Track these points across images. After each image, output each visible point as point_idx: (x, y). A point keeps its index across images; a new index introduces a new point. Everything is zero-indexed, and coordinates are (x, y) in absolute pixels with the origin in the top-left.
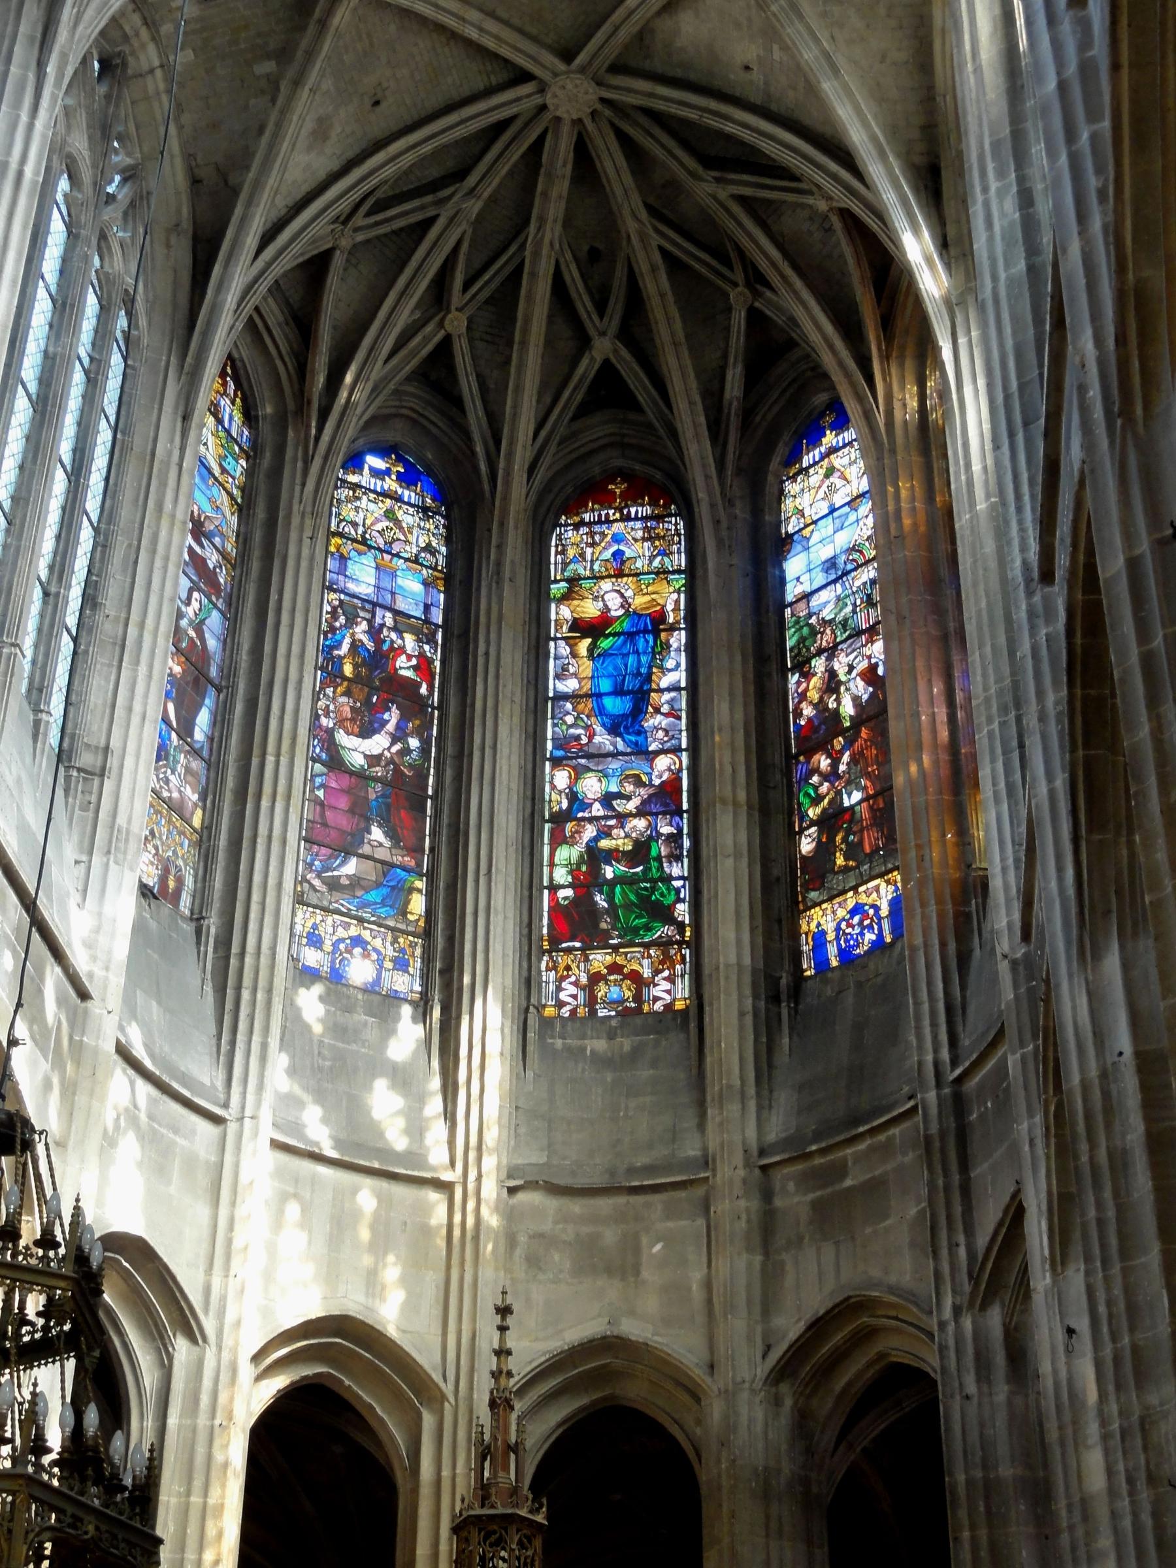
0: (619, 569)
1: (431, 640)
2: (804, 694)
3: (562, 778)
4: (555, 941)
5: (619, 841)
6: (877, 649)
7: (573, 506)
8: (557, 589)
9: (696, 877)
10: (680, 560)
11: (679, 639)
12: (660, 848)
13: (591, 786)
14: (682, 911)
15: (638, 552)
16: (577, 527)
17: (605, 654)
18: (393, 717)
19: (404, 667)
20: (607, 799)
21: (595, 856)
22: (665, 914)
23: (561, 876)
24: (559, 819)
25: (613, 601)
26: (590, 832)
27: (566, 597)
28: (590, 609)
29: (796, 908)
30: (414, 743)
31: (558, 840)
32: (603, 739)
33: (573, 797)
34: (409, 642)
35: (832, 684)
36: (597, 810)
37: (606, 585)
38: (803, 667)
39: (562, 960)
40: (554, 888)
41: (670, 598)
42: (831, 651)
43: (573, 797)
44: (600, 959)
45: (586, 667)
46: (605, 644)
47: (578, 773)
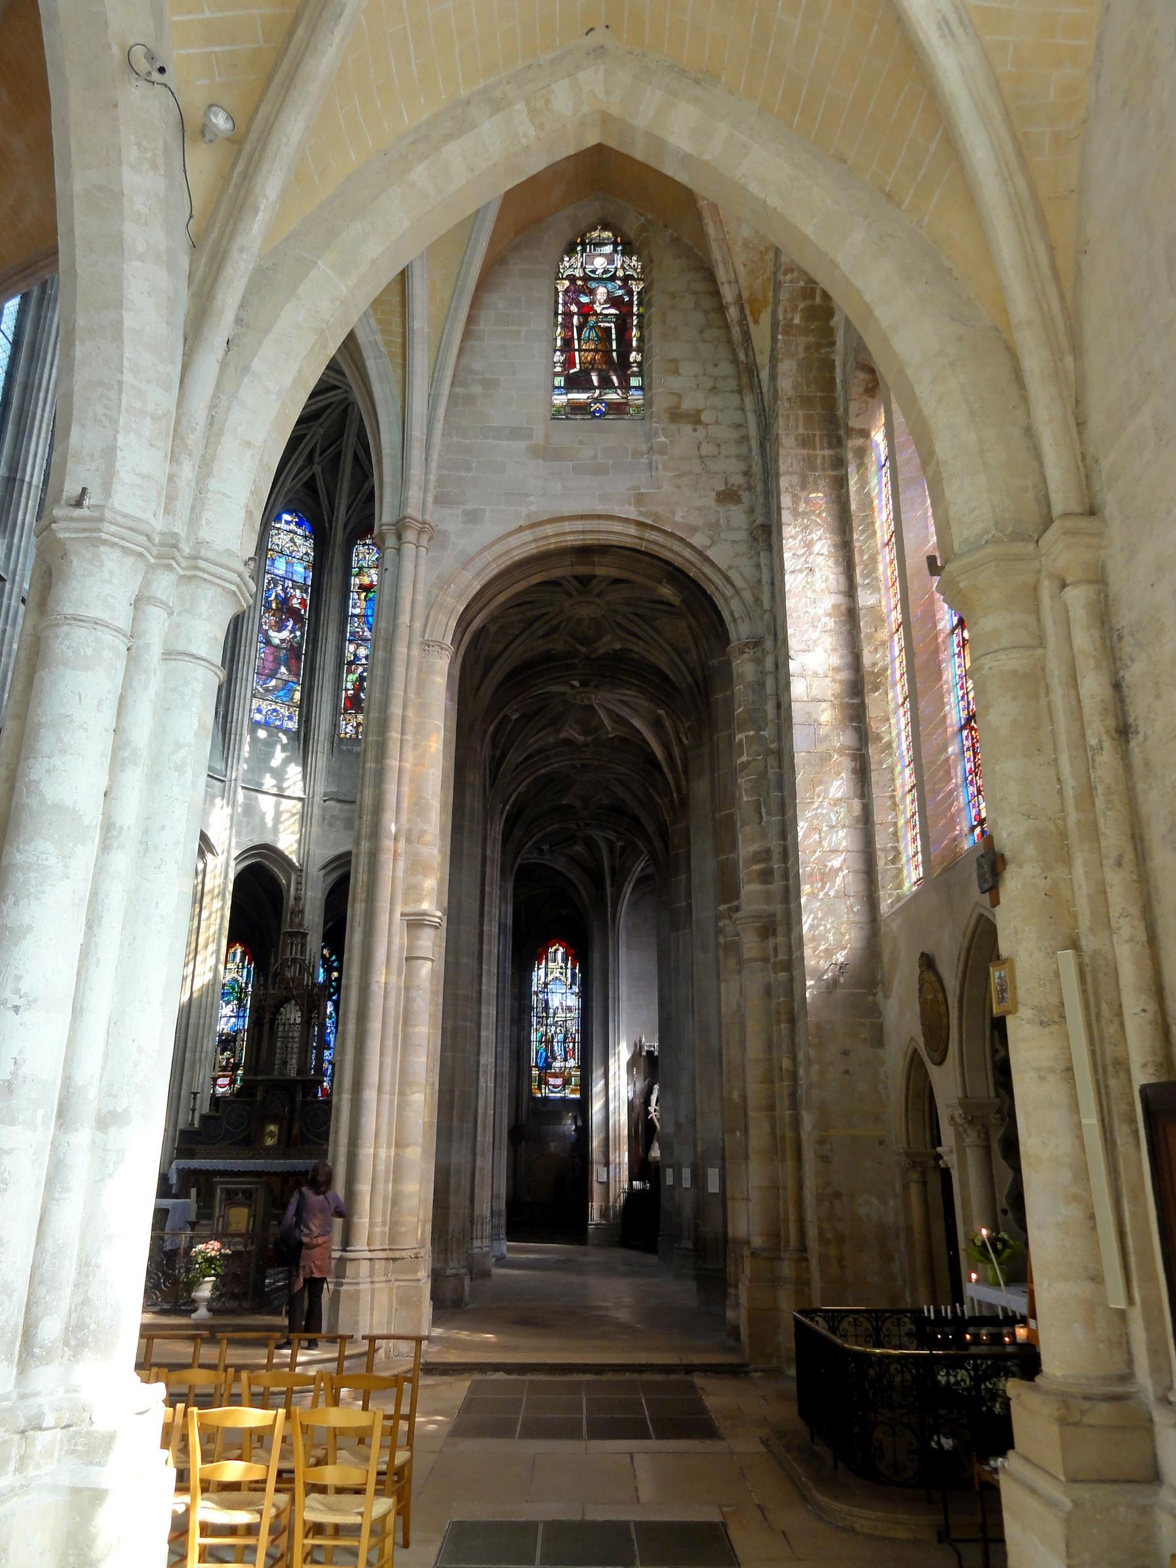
1: (306, 592)
3: (352, 648)
4: (346, 710)
8: (355, 571)
16: (364, 545)
17: (371, 599)
18: (290, 624)
19: (295, 603)
20: (366, 657)
21: (361, 679)
23: (349, 685)
24: (350, 663)
25: (375, 578)
26: (360, 669)
27: (358, 575)
28: (366, 581)
30: (298, 633)
31: (349, 672)
32: (367, 634)
33: (355, 655)
34: (298, 592)
36: (364, 661)
37: (373, 571)
39: (348, 717)
40: (347, 690)
43: (355, 655)
44: (360, 717)
45: (364, 604)
46: (371, 595)
47: (358, 646)
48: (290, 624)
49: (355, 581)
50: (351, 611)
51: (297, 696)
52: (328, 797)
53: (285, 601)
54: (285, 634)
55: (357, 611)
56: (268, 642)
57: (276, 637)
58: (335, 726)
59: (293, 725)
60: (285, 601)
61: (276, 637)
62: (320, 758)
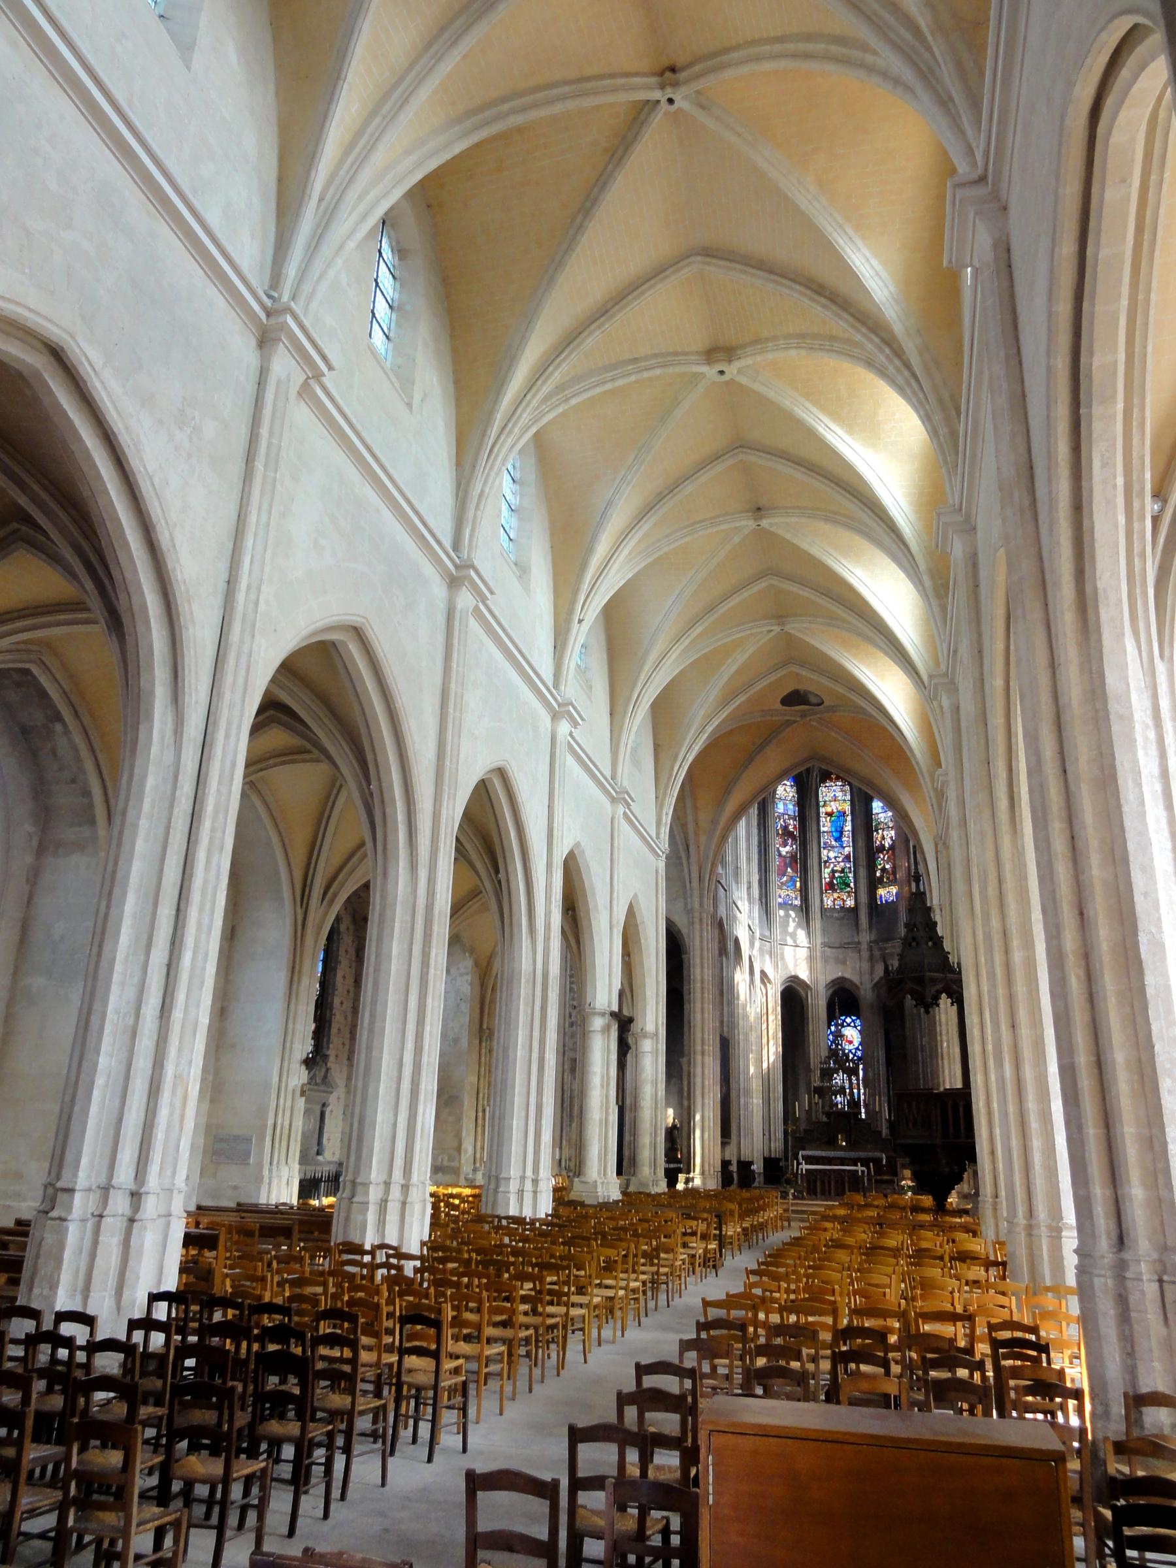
0: (835, 799)
2: (877, 836)
5: (838, 868)
6: (893, 833)
7: (824, 782)
8: (821, 804)
9: (855, 877)
10: (848, 797)
11: (849, 818)
12: (847, 870)
13: (832, 855)
14: (852, 885)
15: (839, 794)
18: (790, 841)
21: (833, 871)
22: (848, 885)
24: (826, 862)
28: (829, 810)
29: (876, 888)
32: (833, 843)
35: (883, 838)
38: (877, 831)
41: (847, 807)
42: (883, 830)
44: (836, 895)
48: (790, 841)
49: (822, 810)
50: (822, 829)
51: (798, 884)
52: (824, 944)
53: (785, 828)
54: (788, 848)
55: (825, 829)
56: (780, 855)
57: (784, 851)
58: (822, 901)
59: (797, 902)
60: (785, 828)
61: (784, 851)
62: (817, 923)
